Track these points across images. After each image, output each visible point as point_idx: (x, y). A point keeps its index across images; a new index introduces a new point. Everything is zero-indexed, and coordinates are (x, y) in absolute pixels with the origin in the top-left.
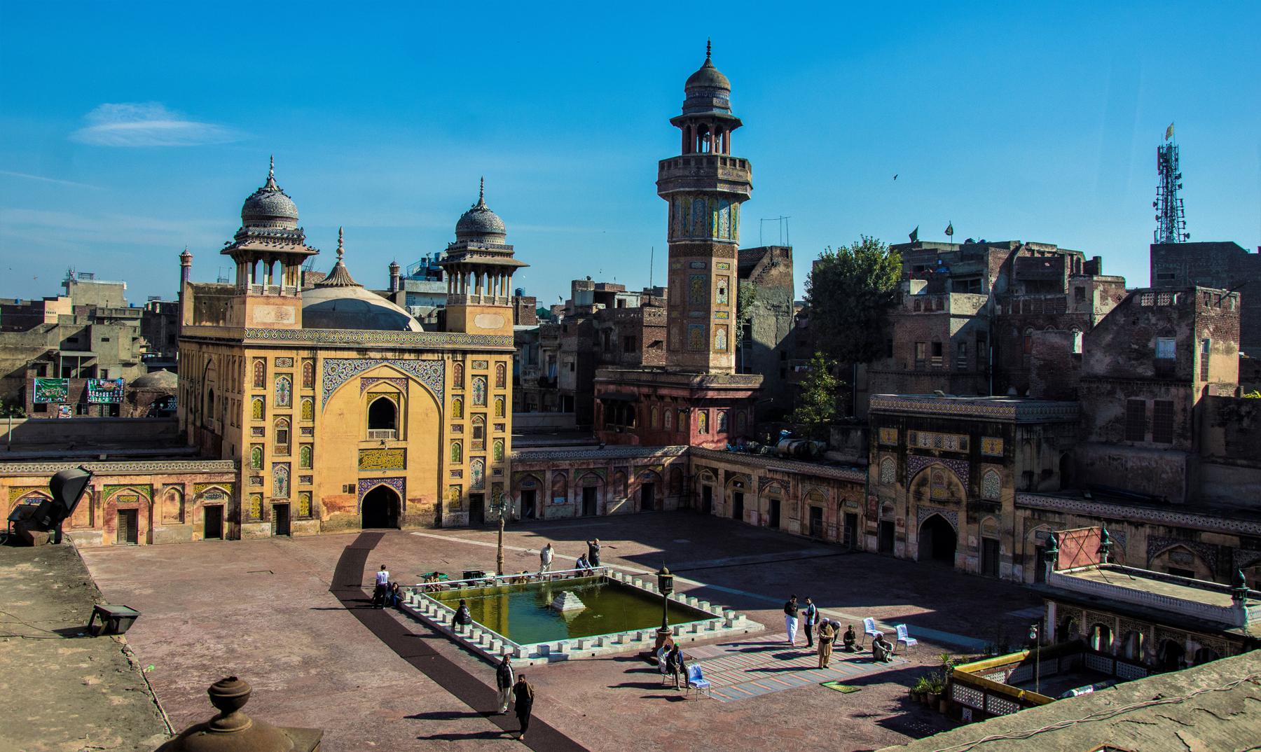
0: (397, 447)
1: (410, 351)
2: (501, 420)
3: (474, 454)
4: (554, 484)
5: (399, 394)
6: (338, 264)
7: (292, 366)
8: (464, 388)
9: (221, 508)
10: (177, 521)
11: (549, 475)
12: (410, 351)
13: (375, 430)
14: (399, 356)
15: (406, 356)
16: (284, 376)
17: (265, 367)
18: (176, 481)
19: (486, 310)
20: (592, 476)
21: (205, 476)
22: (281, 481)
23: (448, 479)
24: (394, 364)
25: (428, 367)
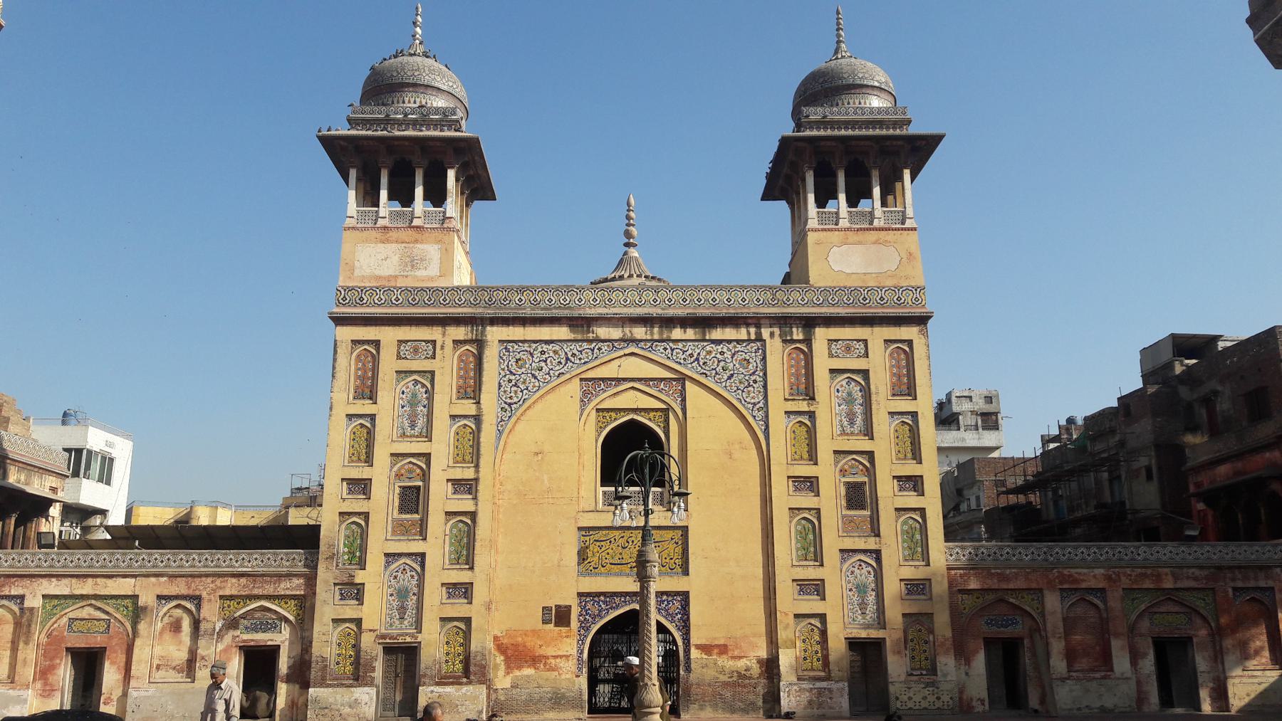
1: (685, 322)
2: (910, 469)
3: (849, 544)
4: (1069, 625)
5: (666, 412)
6: (626, 253)
7: (434, 357)
8: (813, 399)
9: (276, 649)
10: (180, 677)
11: (1052, 602)
12: (685, 322)
14: (661, 333)
15: (677, 333)
16: (416, 377)
17: (375, 360)
18: (184, 591)
19: (852, 237)
20: (1177, 609)
21: (243, 580)
22: (402, 594)
23: (788, 600)
24: (651, 349)
25: (728, 355)
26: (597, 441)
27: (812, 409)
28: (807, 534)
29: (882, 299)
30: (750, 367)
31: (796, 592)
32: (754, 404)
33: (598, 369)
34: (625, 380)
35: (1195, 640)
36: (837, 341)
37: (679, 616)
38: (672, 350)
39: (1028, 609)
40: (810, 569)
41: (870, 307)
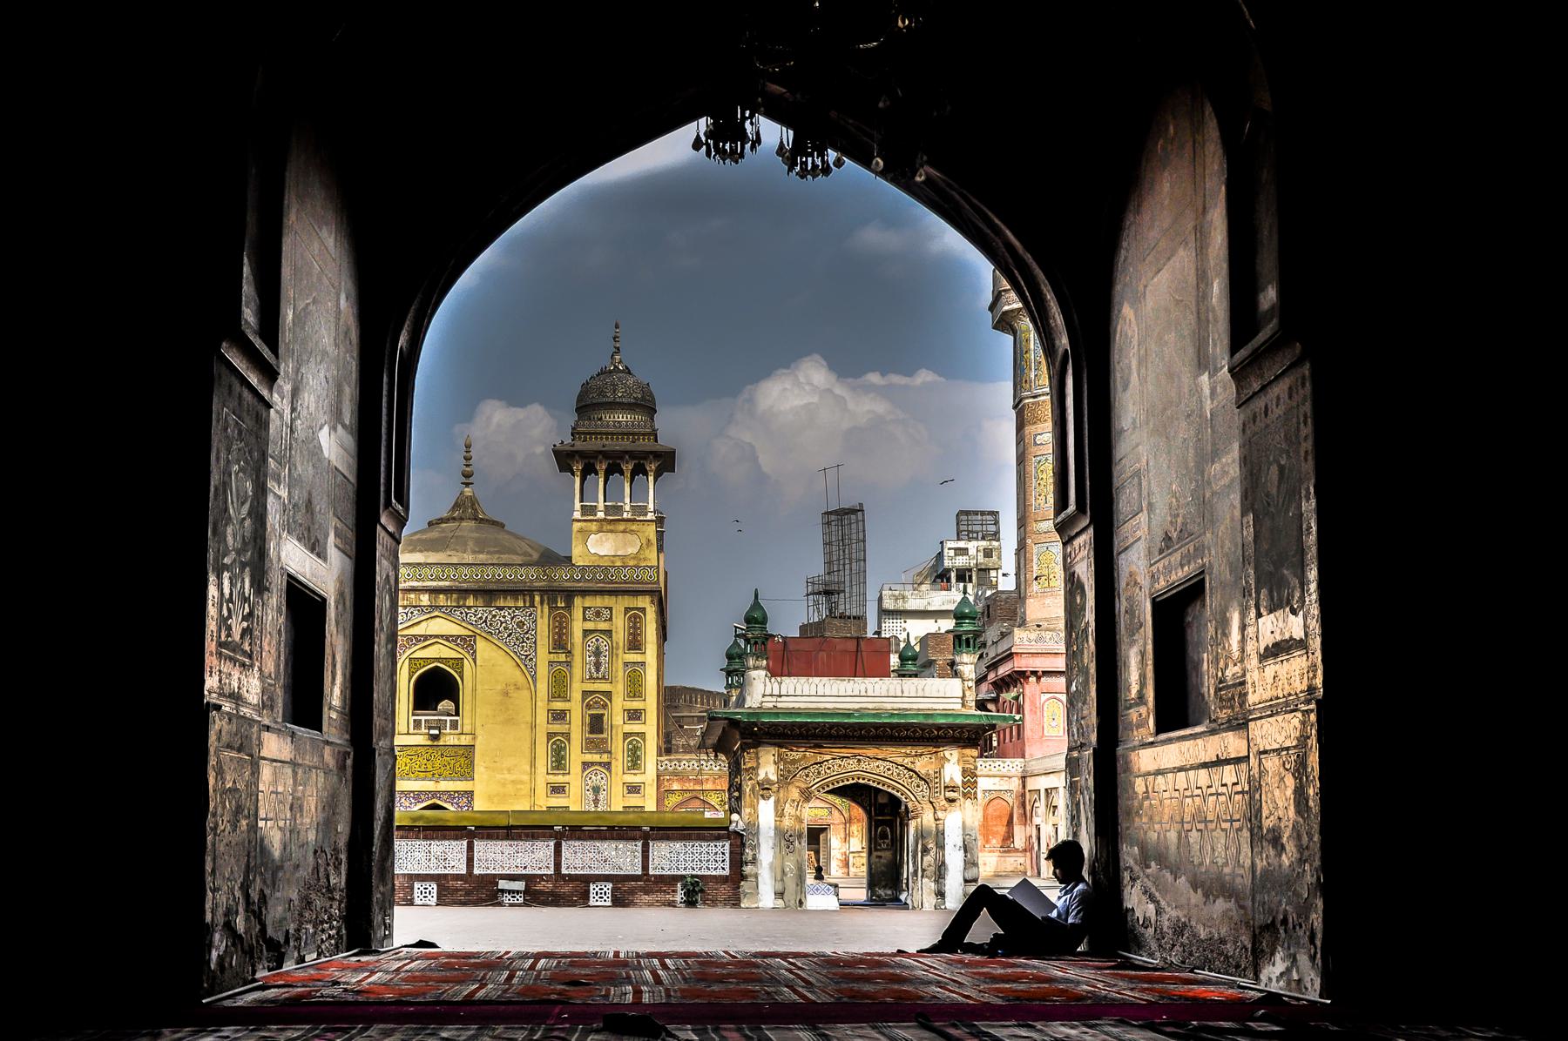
0: (457, 743)
1: (476, 592)
2: (636, 705)
3: (589, 758)
8: (570, 652)
12: (476, 592)
13: (423, 718)
15: (470, 602)
20: (823, 805)
25: (509, 618)
26: (409, 682)
27: (568, 660)
28: (560, 752)
29: (625, 576)
30: (525, 627)
31: (549, 792)
32: (527, 656)
33: (411, 629)
34: (430, 636)
35: (832, 827)
36: (590, 608)
37: (466, 808)
38: (467, 614)
39: (713, 803)
40: (560, 776)
41: (616, 583)
